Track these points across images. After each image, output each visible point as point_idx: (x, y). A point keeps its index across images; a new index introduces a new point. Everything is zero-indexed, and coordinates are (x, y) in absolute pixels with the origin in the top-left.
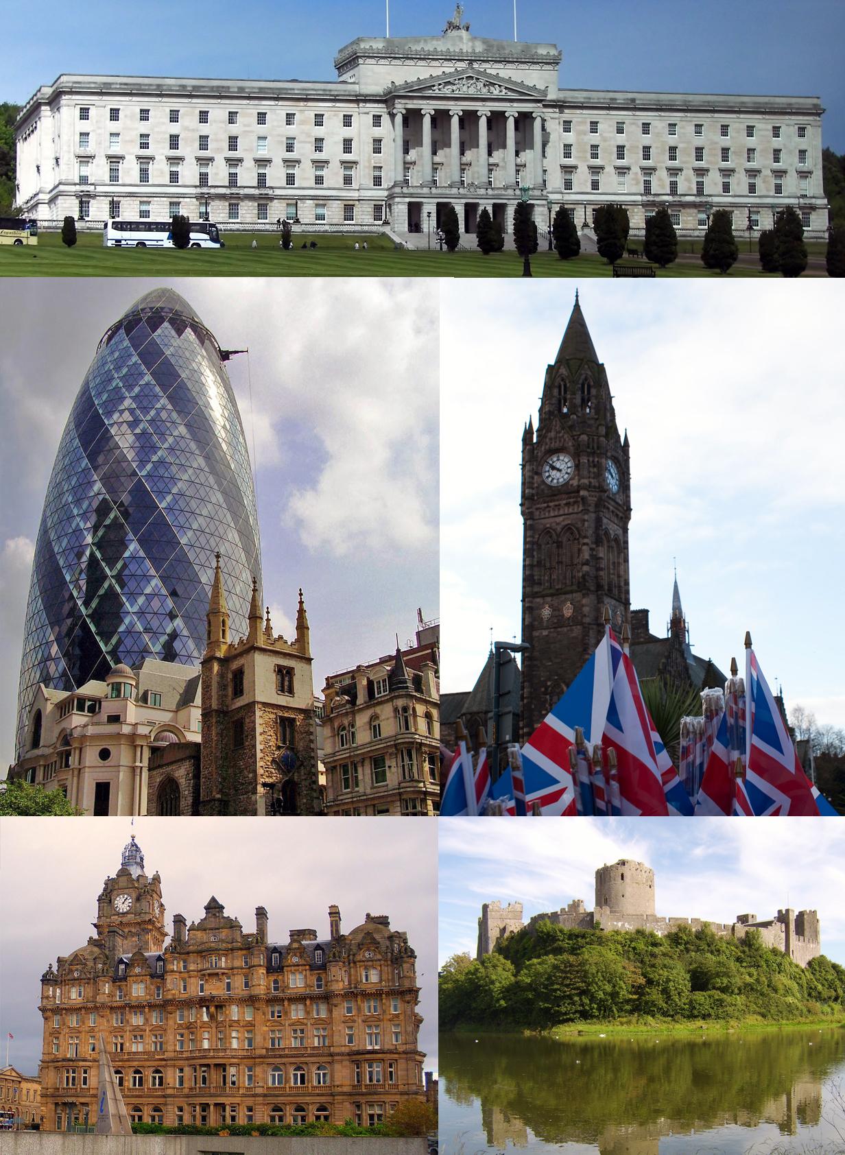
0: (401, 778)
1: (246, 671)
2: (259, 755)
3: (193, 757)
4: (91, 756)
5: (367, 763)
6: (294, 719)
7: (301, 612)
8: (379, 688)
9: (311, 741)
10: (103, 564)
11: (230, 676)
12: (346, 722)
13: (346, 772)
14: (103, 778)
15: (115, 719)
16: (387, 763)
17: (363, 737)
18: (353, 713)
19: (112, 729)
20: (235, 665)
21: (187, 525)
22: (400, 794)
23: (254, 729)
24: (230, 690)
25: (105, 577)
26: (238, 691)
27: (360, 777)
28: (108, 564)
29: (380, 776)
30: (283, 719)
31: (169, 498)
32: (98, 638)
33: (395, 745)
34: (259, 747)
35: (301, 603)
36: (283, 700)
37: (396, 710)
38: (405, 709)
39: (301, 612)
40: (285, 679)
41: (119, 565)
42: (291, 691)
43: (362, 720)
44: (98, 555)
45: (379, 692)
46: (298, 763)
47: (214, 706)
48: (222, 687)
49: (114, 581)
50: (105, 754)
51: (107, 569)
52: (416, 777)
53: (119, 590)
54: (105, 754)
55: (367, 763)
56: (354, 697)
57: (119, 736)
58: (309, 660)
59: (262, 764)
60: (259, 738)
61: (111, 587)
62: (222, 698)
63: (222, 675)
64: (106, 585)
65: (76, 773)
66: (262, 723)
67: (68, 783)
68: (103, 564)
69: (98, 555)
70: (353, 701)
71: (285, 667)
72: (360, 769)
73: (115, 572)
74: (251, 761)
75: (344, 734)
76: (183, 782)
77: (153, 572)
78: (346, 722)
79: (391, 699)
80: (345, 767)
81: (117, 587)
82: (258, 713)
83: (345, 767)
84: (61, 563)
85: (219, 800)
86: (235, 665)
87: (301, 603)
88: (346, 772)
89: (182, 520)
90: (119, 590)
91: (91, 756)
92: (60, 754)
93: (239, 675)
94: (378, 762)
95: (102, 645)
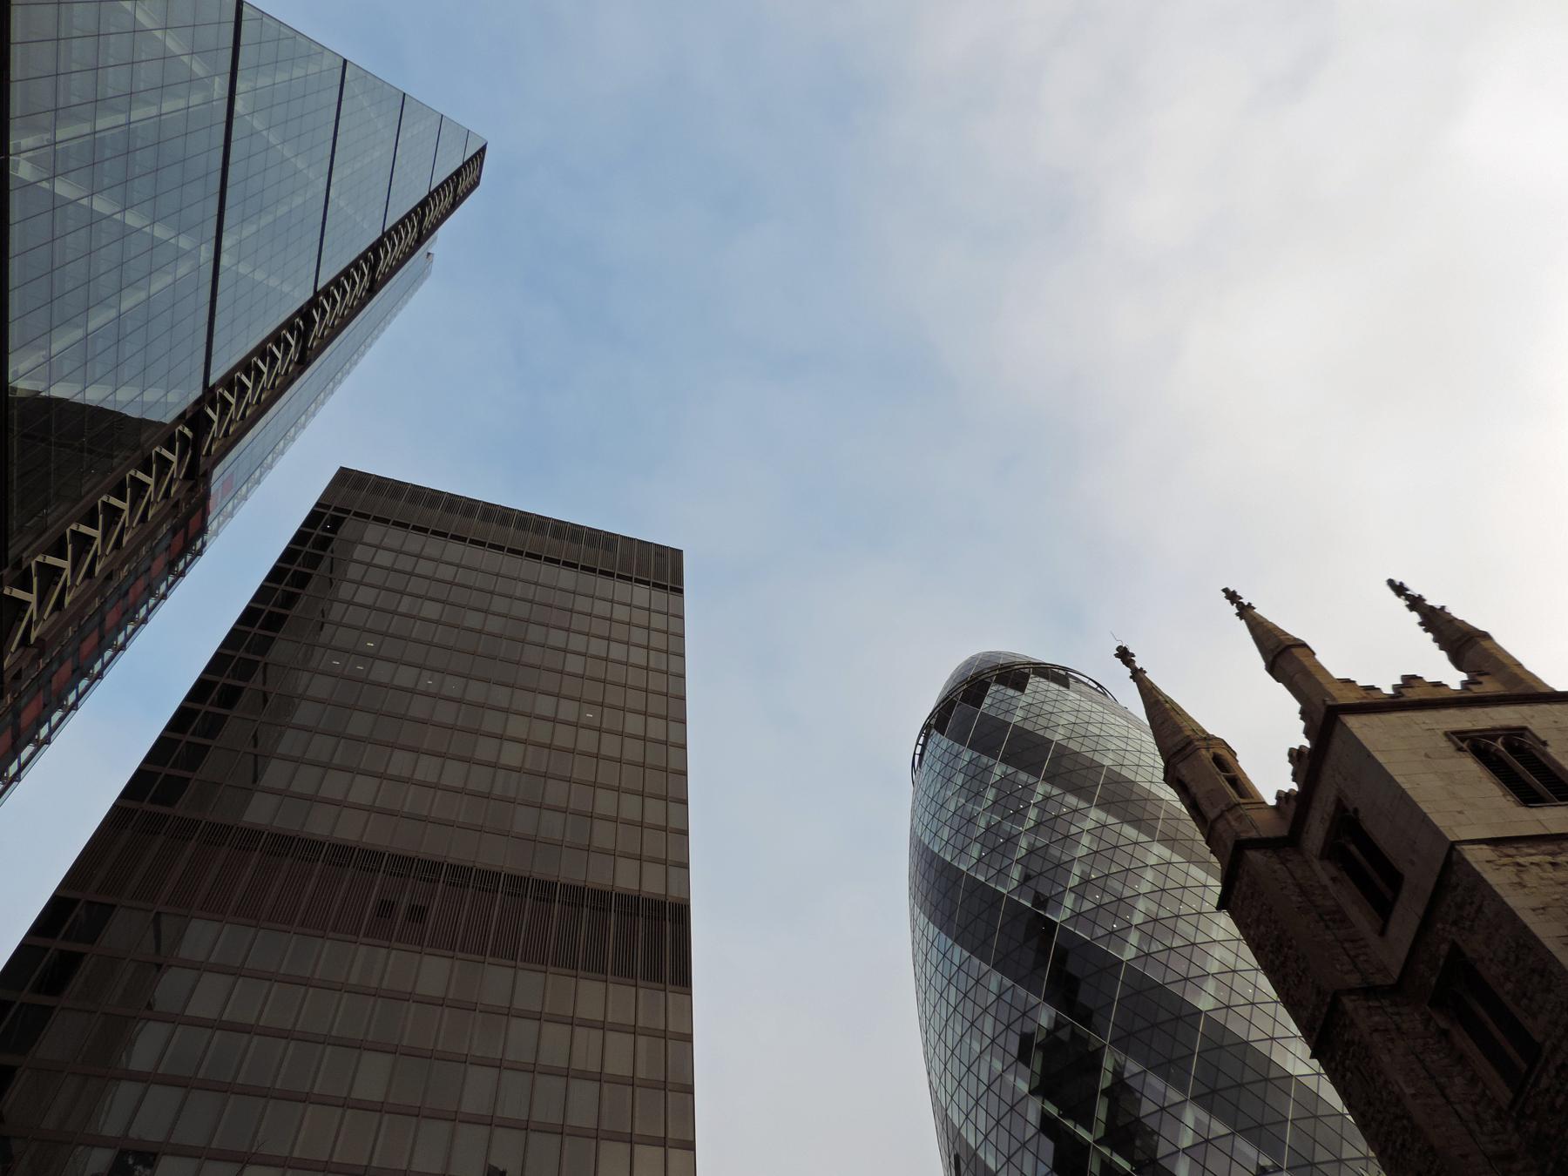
7: (1436, 622)
10: (1070, 1124)
20: (1316, 832)
21: (1194, 971)
24: (1360, 917)
25: (1084, 1148)
28: (1077, 1121)
31: (1134, 938)
35: (1415, 603)
39: (1436, 622)
41: (1101, 1111)
44: (1053, 1110)
49: (1106, 1151)
51: (1082, 1132)
53: (1126, 1166)
68: (1070, 1124)
69: (1053, 1110)
71: (1492, 734)
73: (1100, 1133)
77: (1174, 1096)
81: (1118, 1159)
87: (1415, 603)
89: (1181, 967)
90: (1126, 1166)
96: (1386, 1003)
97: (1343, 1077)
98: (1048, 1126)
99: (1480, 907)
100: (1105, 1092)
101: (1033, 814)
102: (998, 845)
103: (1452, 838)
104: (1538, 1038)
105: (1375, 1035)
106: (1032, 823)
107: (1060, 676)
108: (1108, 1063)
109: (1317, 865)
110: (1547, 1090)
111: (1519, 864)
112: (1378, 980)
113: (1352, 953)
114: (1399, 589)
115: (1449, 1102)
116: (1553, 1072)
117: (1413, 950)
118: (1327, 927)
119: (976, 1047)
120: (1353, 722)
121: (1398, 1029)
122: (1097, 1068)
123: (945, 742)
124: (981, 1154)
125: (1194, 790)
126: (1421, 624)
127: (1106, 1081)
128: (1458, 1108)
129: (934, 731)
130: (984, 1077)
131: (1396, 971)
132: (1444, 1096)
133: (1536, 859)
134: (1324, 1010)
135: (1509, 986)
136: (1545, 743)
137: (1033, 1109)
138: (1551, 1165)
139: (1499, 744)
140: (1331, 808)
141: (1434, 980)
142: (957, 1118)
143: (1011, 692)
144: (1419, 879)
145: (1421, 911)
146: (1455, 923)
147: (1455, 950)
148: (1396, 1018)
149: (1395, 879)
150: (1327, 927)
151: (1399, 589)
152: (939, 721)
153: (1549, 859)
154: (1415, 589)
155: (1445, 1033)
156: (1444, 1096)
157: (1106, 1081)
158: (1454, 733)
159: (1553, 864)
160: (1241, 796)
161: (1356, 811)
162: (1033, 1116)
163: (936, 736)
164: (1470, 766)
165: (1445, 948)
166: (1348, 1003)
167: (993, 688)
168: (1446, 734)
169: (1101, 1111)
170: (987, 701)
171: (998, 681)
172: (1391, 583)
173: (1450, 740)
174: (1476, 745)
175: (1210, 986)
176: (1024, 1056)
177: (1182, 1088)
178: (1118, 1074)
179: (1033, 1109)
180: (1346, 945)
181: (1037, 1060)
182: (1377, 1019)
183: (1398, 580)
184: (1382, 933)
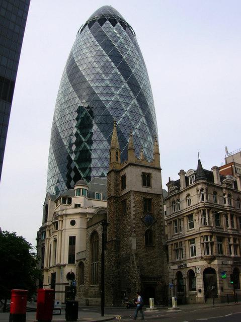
0: (201, 226)
2: (133, 217)
5: (185, 218)
6: (151, 199)
8: (191, 180)
9: (161, 210)
12: (175, 199)
13: (176, 224)
14: (72, 234)
15: (78, 206)
16: (194, 218)
17: (184, 206)
18: (179, 194)
19: (78, 210)
20: (122, 174)
21: (120, 115)
22: (200, 233)
23: (130, 205)
26: (124, 187)
27: (182, 226)
29: (192, 225)
30: (145, 199)
32: (80, 171)
33: (198, 209)
34: (133, 213)
36: (145, 190)
37: (198, 190)
38: (202, 190)
40: (147, 180)
41: (88, 136)
43: (183, 196)
44: (79, 132)
45: (191, 183)
46: (154, 221)
47: (112, 195)
48: (116, 185)
49: (86, 144)
50: (73, 223)
52: (208, 224)
54: (73, 223)
55: (185, 218)
56: (179, 186)
57: (80, 213)
58: (160, 169)
59: (134, 221)
60: (133, 209)
61: (85, 146)
62: (116, 190)
63: (116, 180)
64: (83, 146)
65: (60, 232)
66: (132, 201)
67: (57, 237)
69: (79, 132)
70: (179, 189)
72: (182, 222)
73: (87, 140)
75: (175, 204)
78: (175, 199)
79: (195, 185)
80: (175, 221)
82: (132, 197)
83: (175, 221)
84: (62, 137)
85: (115, 241)
86: (122, 174)
88: (176, 224)
92: (54, 223)
93: (124, 177)
94: (190, 217)
95: (82, 174)
98: (77, 135)
107: (125, 25)
119: (68, 112)
123: (89, 32)
124: (61, 134)
129: (87, 26)
130: (67, 119)
137: (75, 130)
142: (58, 124)
143: (111, 26)
152: (90, 24)
163: (88, 31)
164: (141, 179)
167: (108, 22)
170: (104, 25)
171: (110, 20)
174: (144, 175)
175: (121, 119)
176: (77, 119)
177: (106, 138)
179: (75, 130)
181: (80, 121)
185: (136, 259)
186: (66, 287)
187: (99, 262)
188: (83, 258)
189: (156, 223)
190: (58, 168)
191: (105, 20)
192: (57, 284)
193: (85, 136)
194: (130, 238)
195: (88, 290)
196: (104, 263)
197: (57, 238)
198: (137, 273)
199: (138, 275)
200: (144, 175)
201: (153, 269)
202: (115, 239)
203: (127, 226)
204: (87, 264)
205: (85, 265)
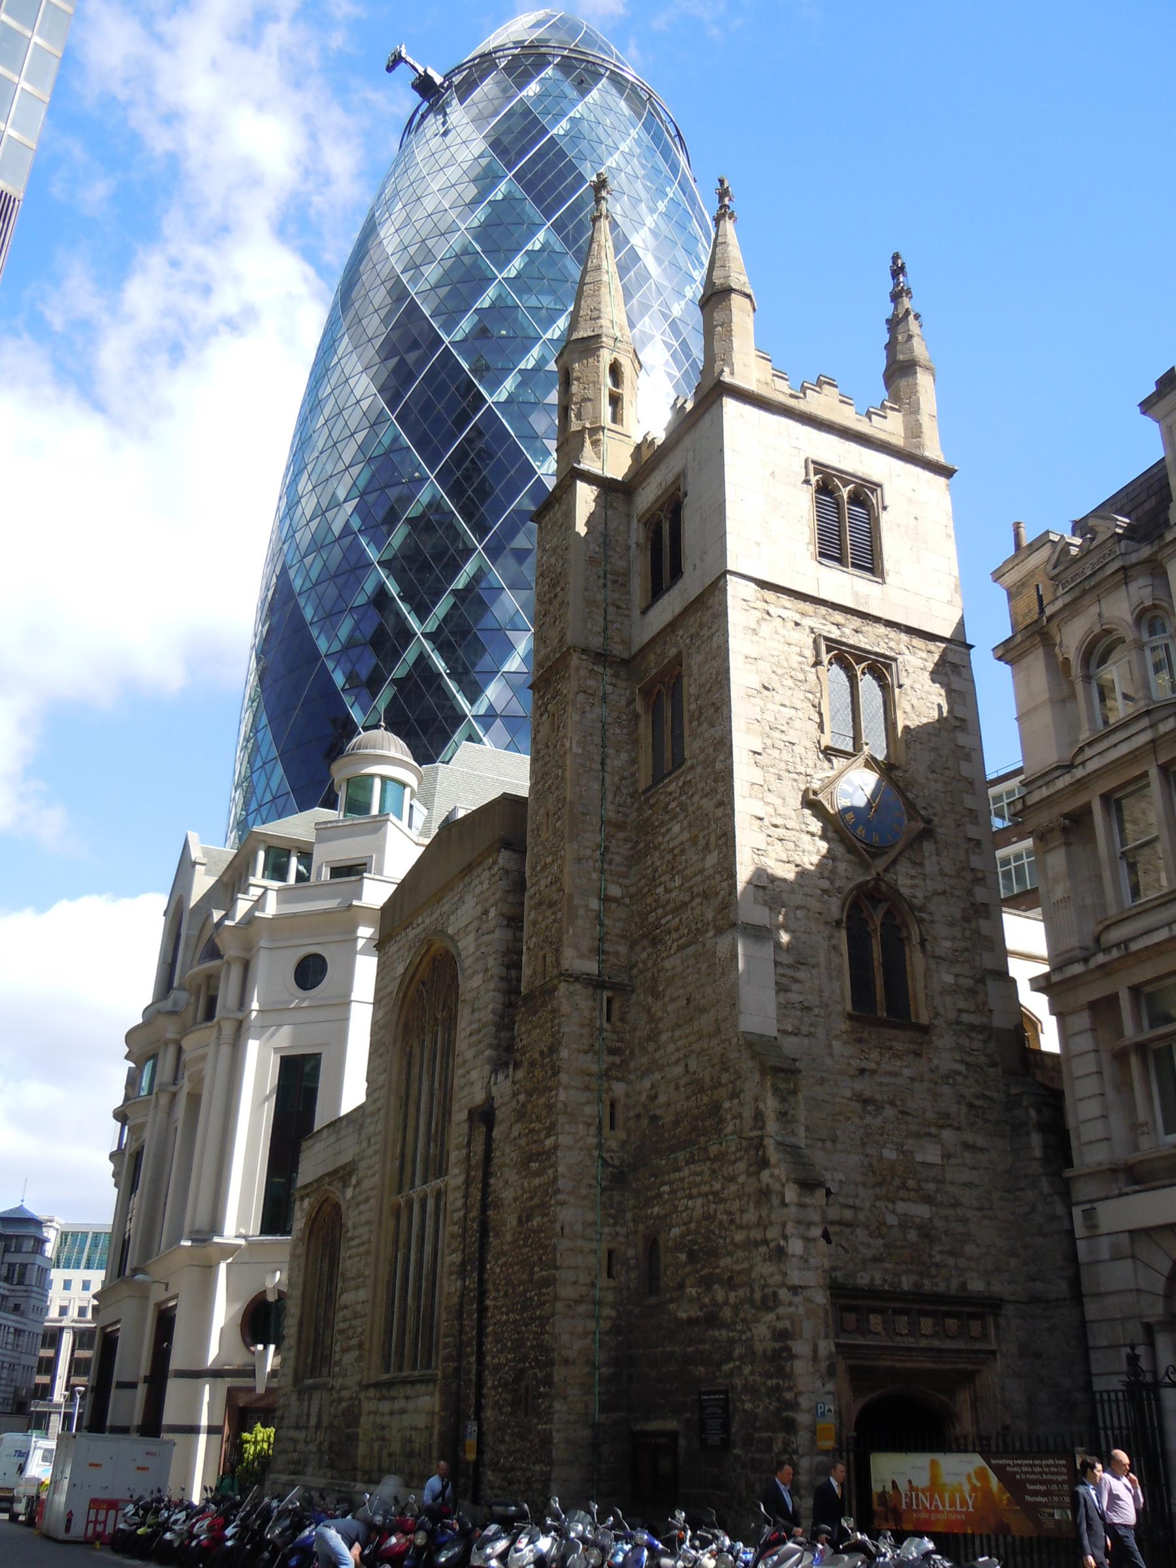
1: (693, 487)
3: (507, 844)
4: (272, 974)
11: (637, 534)
41: (441, 608)
42: (869, 561)
44: (393, 588)
49: (428, 646)
50: (310, 972)
53: (440, 665)
61: (422, 658)
64: (410, 655)
65: (228, 1029)
68: (404, 608)
69: (393, 588)
71: (845, 477)
73: (431, 625)
74: (707, 804)
76: (467, 946)
90: (440, 665)
91: (272, 974)
96: (609, 671)
97: (542, 715)
99: (713, 635)
100: (455, 592)
101: (518, 263)
102: (465, 279)
103: (730, 567)
104: (687, 754)
105: (581, 697)
106: (513, 274)
108: (469, 568)
109: (634, 524)
110: (671, 794)
111: (768, 613)
112: (617, 650)
113: (609, 618)
114: (898, 271)
115: (603, 770)
116: (681, 784)
117: (653, 640)
118: (605, 585)
120: (730, 406)
121: (604, 698)
122: (455, 569)
125: (575, 388)
126: (888, 321)
127: (460, 582)
128: (606, 775)
131: (635, 648)
132: (603, 764)
133: (785, 614)
134: (557, 656)
135: (693, 707)
136: (885, 508)
138: (642, 845)
139: (845, 492)
140: (670, 478)
141: (654, 671)
144: (690, 586)
145: (677, 610)
146: (692, 637)
147: (678, 660)
148: (609, 689)
149: (677, 572)
150: (605, 585)
151: (898, 271)
153: (797, 618)
154: (909, 280)
155: (637, 716)
156: (603, 764)
157: (460, 582)
158: (814, 462)
159: (797, 624)
160: (615, 419)
161: (685, 494)
162: (369, 586)
165: (673, 652)
166: (575, 660)
168: (806, 461)
169: (441, 608)
171: (566, 66)
172: (896, 257)
173: (806, 467)
174: (825, 483)
178: (479, 576)
180: (611, 609)
182: (591, 682)
183: (905, 259)
184: (644, 612)
185: (782, 1115)
186: (231, 1393)
187: (455, 1178)
188: (341, 1161)
189: (928, 847)
190: (279, 771)
191: (541, 62)
192: (182, 1374)
193: (422, 613)
194: (722, 946)
195: (352, 1416)
196: (487, 1175)
197: (208, 1073)
198: (795, 1247)
199: (811, 1278)
200: (825, 483)
201: (926, 1232)
202: (592, 967)
203: (692, 854)
204: (363, 1219)
205: (351, 1218)
